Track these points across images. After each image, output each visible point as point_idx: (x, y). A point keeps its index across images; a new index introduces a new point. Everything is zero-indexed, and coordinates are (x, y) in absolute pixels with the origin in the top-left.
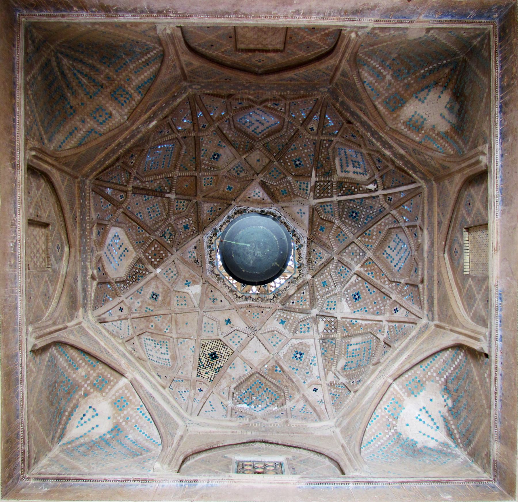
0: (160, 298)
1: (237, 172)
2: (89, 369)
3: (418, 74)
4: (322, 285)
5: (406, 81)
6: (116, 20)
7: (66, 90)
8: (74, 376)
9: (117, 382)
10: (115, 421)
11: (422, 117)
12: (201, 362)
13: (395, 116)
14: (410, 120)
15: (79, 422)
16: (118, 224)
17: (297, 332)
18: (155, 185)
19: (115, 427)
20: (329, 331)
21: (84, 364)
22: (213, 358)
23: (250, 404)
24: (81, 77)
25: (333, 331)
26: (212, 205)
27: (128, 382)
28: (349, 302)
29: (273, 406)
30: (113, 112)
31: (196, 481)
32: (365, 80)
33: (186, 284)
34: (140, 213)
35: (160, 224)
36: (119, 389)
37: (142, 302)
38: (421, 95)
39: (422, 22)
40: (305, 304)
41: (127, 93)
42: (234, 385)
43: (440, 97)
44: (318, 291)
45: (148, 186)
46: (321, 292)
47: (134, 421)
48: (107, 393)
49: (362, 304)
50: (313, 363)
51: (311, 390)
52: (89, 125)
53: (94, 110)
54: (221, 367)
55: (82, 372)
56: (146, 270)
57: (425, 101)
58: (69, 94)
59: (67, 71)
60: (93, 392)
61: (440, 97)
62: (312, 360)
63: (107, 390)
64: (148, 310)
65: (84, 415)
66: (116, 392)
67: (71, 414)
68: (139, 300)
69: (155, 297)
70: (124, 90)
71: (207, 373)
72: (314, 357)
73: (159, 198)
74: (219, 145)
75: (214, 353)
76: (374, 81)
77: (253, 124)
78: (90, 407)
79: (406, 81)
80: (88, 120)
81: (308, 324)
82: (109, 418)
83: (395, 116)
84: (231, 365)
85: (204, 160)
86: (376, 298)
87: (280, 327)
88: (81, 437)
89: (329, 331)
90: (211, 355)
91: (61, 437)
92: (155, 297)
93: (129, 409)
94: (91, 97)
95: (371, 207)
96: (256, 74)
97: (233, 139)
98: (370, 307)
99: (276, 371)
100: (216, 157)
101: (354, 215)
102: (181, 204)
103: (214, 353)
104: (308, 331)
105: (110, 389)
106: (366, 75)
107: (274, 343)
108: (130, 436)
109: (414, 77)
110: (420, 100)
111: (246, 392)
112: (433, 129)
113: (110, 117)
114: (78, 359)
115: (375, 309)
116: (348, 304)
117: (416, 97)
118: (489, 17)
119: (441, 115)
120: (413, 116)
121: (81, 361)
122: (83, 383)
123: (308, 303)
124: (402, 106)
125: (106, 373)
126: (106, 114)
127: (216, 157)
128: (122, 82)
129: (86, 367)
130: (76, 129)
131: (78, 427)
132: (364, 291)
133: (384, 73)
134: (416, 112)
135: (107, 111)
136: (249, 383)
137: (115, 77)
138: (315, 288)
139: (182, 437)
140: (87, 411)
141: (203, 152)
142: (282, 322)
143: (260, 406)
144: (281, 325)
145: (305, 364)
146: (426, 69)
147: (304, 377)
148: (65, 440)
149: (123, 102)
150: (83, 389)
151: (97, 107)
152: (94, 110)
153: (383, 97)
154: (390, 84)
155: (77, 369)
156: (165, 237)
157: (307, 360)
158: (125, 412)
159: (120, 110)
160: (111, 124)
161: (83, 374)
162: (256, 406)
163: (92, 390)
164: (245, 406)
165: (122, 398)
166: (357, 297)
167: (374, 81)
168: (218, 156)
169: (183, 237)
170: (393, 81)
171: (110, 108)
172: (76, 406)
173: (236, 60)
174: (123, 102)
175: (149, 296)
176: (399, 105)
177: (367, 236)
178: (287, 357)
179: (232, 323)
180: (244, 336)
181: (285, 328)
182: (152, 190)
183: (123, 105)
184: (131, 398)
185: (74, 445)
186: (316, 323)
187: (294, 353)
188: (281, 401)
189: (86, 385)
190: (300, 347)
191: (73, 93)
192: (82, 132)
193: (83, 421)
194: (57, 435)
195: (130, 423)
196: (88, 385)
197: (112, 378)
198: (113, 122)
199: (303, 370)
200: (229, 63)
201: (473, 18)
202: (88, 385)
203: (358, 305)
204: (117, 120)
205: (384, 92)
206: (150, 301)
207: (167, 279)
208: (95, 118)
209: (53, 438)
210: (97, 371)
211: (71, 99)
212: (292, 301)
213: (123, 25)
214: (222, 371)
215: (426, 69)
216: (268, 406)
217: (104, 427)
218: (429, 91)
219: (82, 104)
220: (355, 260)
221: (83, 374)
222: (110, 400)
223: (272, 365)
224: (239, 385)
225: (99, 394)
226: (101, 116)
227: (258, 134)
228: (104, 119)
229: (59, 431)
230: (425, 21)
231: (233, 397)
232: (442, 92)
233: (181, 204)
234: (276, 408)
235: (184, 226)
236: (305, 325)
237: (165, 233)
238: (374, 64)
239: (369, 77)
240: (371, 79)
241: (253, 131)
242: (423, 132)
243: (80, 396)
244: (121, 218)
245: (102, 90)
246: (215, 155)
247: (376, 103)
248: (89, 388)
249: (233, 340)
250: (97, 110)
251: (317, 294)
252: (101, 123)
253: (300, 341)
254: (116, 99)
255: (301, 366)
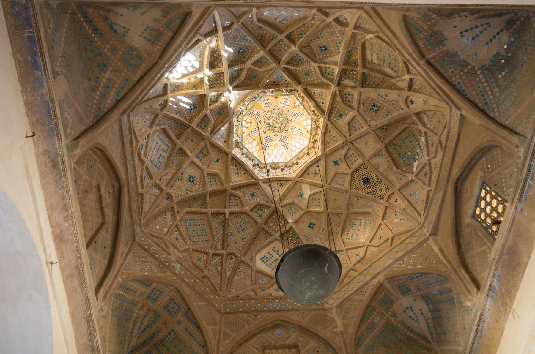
0: (313, 221)
1: (203, 157)
2: (375, 313)
3: (99, 43)
4: (308, 77)
5: (109, 54)
6: (100, 347)
7: (157, 340)
8: (380, 326)
9: (387, 289)
10: (419, 297)
11: (145, 30)
12: (371, 192)
13: (146, 55)
14: (149, 40)
15: (415, 322)
16: (252, 259)
17: (352, 105)
18: (219, 228)
19: (424, 298)
20: (355, 76)
21: (371, 318)
22: (368, 182)
23: (414, 158)
24: (143, 326)
25: (355, 73)
26: (233, 173)
27: (388, 281)
28: (328, 55)
29: (420, 140)
30: (168, 297)
31: (491, 285)
32: (114, 100)
33: (302, 197)
34: (243, 239)
35: (251, 220)
36: (392, 287)
37: (316, 237)
38: (120, 31)
39: (49, 88)
40: (326, 93)
41: (152, 291)
42: (395, 168)
43: (122, 15)
44: (314, 80)
45: (220, 234)
46: (315, 78)
47: (421, 285)
48: (395, 298)
49: (331, 45)
50: (384, 97)
51: (412, 106)
52: (182, 318)
53: (168, 313)
54: (377, 176)
55: (377, 319)
56: (289, 230)
57: (127, 27)
58: (159, 336)
59: (141, 339)
60: (393, 309)
61: (122, 15)
62: (382, 97)
63: (393, 297)
64: (323, 233)
65: (410, 317)
66: (395, 290)
67: (408, 328)
68: (315, 240)
69: (312, 226)
70: (150, 294)
71: (381, 190)
72: (379, 95)
73: (230, 222)
74: (181, 180)
75: (364, 179)
76: (114, 89)
77: (160, 155)
78: (405, 312)
79: (109, 54)
80: (178, 318)
81: (345, 94)
82: (415, 300)
83: (146, 55)
84: (376, 167)
85: (195, 190)
86: (329, 33)
87: (346, 119)
88: (427, 323)
89: (355, 76)
90: (365, 183)
91: (427, 341)
92: (312, 226)
93: (411, 285)
94: (159, 316)
95: (235, 38)
96: (120, 189)
97: (175, 168)
98: (336, 39)
99: (386, 129)
100: (192, 179)
101: (241, 51)
102: (234, 202)
103: (364, 179)
104: (352, 95)
105: (392, 295)
106: (109, 101)
107: (360, 126)
108: (434, 293)
109: (103, 46)
110: (127, 32)
111: (402, 159)
112: (157, 20)
113: (173, 300)
114: (367, 324)
115: (338, 35)
116: (330, 56)
117: (124, 36)
118: (26, 8)
119: (141, 14)
120: (145, 38)
121: (369, 321)
122: (386, 318)
123: (325, 91)
124: (135, 49)
125: (379, 298)
126: (171, 303)
127: (192, 179)
128: (144, 297)
129: (373, 316)
130: (186, 330)
131: (419, 323)
132: (319, 42)
133: (104, 81)
134: (140, 36)
135: (169, 303)
136: (394, 155)
137: (140, 304)
138: (310, 82)
139: (441, 250)
140: (408, 314)
141: (188, 192)
142: (341, 116)
143: (418, 151)
144: (343, 118)
145: (384, 104)
146: (93, 36)
147: (397, 108)
148: (428, 336)
149: (159, 292)
150: (390, 318)
151: (166, 310)
152: (168, 313)
153: (129, 73)
154: (115, 70)
155: (374, 324)
156: (262, 214)
157: (381, 102)
158: (412, 288)
159: (166, 292)
160: (179, 300)
161: (378, 318)
162: (417, 154)
163: (392, 310)
164: (416, 164)
165: (400, 287)
166: (324, 49)
167: (114, 89)
168: (190, 177)
169: (261, 198)
170: (110, 69)
171: (166, 300)
172: (403, 324)
173: (111, 214)
174: (159, 292)
175: (311, 231)
176: (134, 52)
177: (263, 39)
178: (375, 119)
179: (338, 160)
180: (351, 152)
181: (346, 115)
182: (224, 231)
183: (162, 292)
184: (401, 282)
185: (434, 332)
186: (346, 86)
187: (371, 111)
188: (416, 132)
189: (388, 315)
190: (367, 105)
191: (158, 332)
192: (188, 325)
193: (415, 319)
194: (425, 343)
195: (423, 288)
196: (387, 313)
197: (383, 293)
198: (177, 297)
199: (390, 107)
200: (115, 218)
201: (31, 27)
202: (387, 313)
203: (333, 49)
204: (175, 295)
205: (123, 74)
206: (316, 229)
207: (297, 213)
208: (175, 313)
209: (427, 349)
210: (377, 306)
211: (162, 334)
212: (321, 104)
213: (103, 338)
214: (380, 177)
215: (93, 36)
216: (418, 144)
217: (421, 306)
218: (116, 24)
219: (165, 323)
220: (286, 48)
221: (378, 318)
222: (401, 296)
223: (380, 132)
224: (395, 163)
225: (395, 304)
226: (173, 308)
227: (169, 147)
228: (175, 305)
229: (421, 341)
230: (48, 85)
231: (405, 172)
232: (116, 14)
233: (234, 202)
234: (422, 138)
235: (252, 197)
236: (346, 97)
237: (258, 214)
238: (97, 98)
239: (110, 97)
240: (112, 93)
241: (166, 152)
242: (161, 29)
243: (395, 320)
244: (248, 256)
245: (151, 309)
246: (190, 181)
247: (136, 79)
248: (390, 313)
249: (353, 161)
250: (168, 311)
251: (316, 81)
252: (179, 308)
253: (361, 104)
254: (158, 297)
255: (385, 108)
